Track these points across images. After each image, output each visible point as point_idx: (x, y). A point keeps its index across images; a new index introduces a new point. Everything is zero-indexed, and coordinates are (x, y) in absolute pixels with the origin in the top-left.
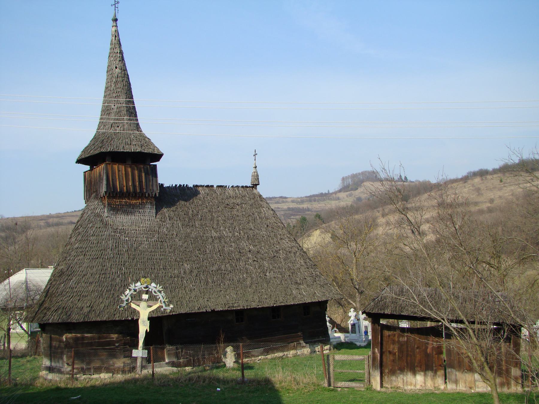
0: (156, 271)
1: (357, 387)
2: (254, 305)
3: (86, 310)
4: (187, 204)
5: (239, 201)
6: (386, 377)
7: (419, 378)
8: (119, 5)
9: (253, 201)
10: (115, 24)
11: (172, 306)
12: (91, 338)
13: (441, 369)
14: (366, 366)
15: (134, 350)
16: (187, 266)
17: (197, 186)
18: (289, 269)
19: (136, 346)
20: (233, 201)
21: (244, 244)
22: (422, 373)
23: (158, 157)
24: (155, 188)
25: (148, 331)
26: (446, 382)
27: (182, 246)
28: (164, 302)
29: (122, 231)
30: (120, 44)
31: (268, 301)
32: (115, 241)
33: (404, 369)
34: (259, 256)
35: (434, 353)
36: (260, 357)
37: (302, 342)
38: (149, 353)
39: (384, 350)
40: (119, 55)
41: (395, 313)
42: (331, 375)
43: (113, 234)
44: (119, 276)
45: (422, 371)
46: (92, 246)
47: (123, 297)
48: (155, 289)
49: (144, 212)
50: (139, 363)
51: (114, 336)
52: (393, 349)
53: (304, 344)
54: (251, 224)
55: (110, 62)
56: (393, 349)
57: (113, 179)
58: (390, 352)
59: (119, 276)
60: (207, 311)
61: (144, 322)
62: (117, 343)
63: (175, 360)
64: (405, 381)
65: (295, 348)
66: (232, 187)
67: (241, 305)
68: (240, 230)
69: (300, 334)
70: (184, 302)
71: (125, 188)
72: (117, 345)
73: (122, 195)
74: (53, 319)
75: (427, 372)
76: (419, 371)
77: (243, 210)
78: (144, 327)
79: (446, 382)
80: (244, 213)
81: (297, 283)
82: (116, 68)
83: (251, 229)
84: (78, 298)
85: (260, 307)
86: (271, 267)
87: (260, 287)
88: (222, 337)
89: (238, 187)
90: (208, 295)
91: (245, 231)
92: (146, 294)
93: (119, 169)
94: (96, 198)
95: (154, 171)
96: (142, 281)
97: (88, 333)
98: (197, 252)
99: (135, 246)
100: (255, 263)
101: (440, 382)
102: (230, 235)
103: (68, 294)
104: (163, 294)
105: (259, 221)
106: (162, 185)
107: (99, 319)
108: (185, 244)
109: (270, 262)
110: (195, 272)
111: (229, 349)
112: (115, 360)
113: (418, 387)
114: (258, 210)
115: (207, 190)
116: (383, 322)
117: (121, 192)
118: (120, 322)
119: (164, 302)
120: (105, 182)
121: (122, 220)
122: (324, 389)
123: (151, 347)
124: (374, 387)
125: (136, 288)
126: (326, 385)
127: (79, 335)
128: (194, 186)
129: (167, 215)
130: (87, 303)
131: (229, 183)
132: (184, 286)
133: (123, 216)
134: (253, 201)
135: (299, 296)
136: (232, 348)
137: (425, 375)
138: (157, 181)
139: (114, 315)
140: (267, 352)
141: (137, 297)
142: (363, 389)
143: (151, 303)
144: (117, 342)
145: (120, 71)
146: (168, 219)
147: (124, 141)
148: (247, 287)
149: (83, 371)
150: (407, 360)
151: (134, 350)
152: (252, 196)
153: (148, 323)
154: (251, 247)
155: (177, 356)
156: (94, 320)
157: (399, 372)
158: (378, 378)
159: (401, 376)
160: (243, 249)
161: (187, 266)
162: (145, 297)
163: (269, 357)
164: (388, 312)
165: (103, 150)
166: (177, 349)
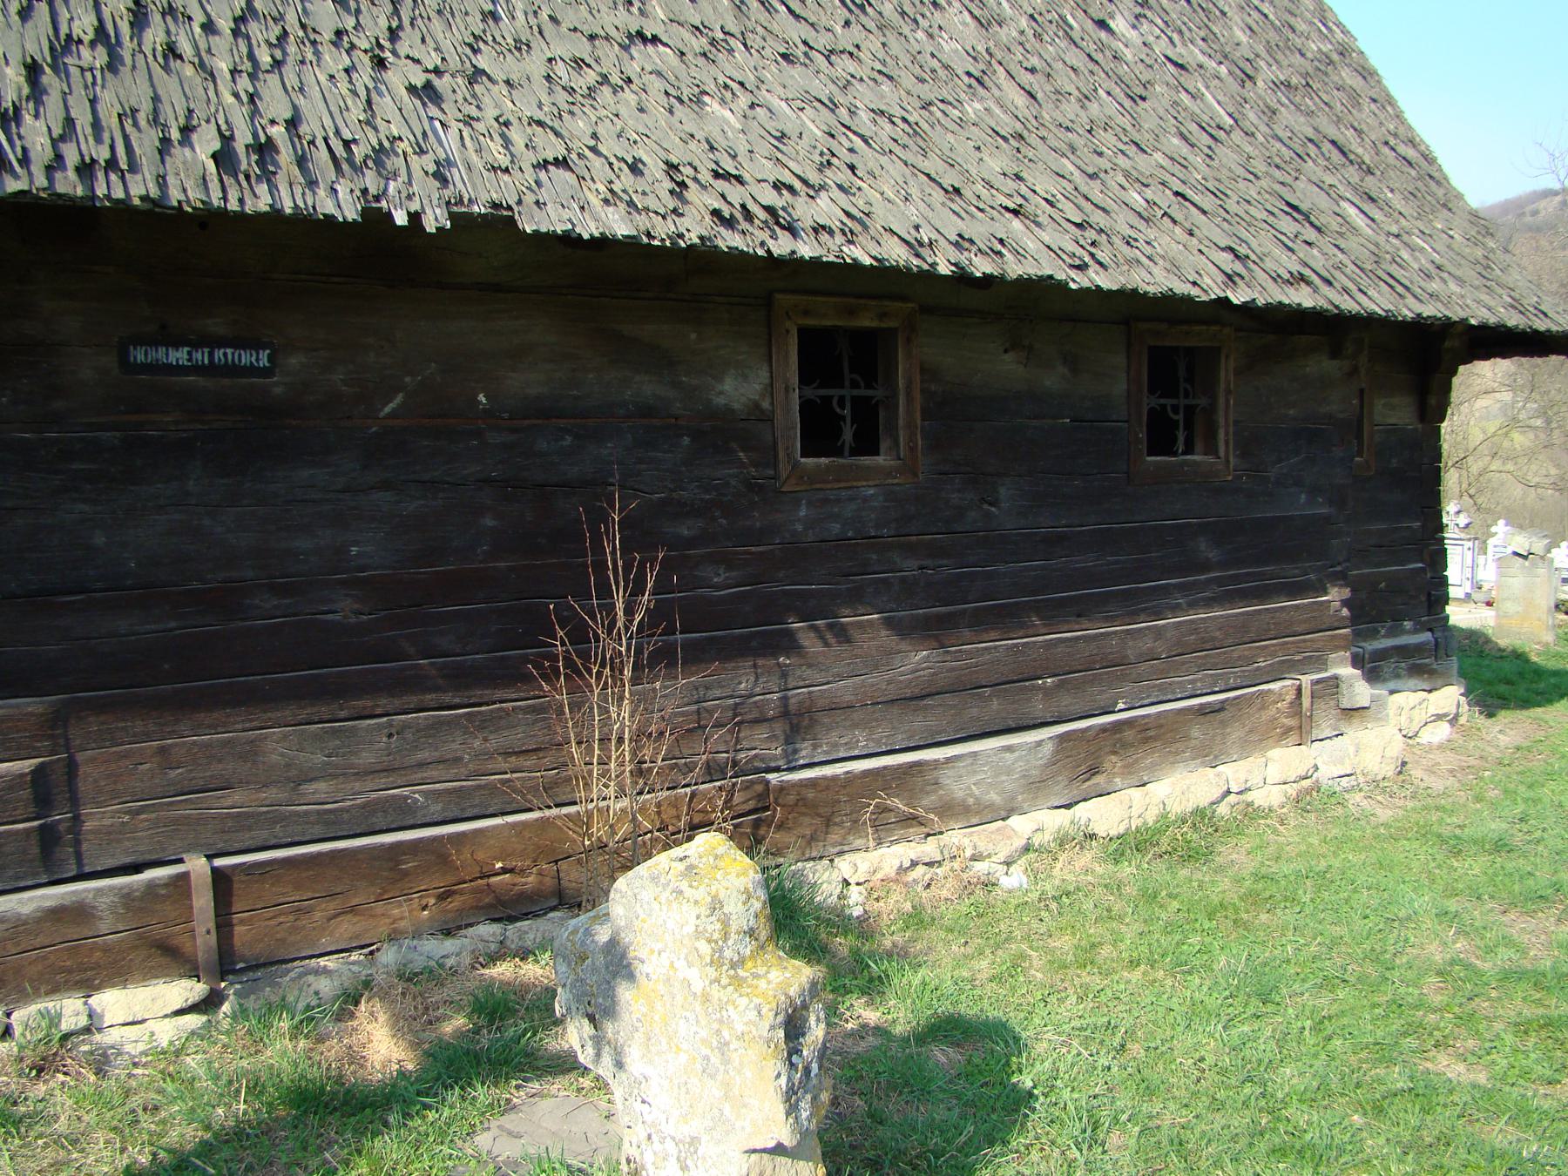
2: (1035, 254)
36: (1022, 826)
53: (1360, 691)
60: (374, 219)
65: (1299, 728)
69: (1335, 596)
85: (1106, 282)
88: (624, 616)
140: (1085, 766)
163: (1108, 814)
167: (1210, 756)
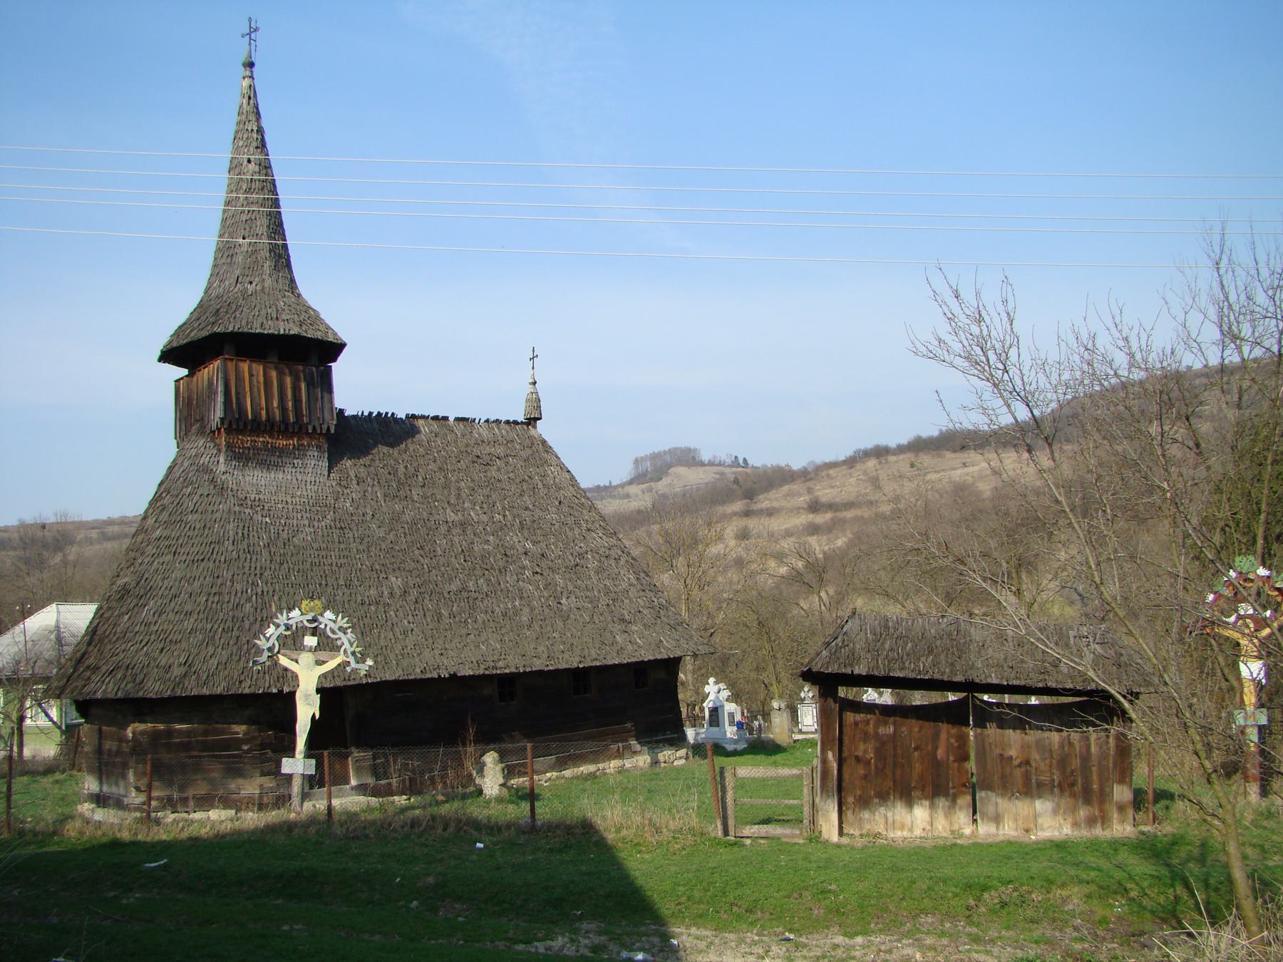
0: (330, 589)
1: (786, 836)
2: (538, 665)
3: (177, 671)
4: (395, 452)
5: (500, 451)
6: (849, 813)
7: (920, 813)
8: (258, 36)
9: (529, 451)
10: (248, 73)
11: (370, 662)
12: (188, 733)
13: (965, 793)
14: (806, 791)
15: (284, 760)
16: (396, 582)
17: (414, 416)
18: (607, 592)
19: (290, 751)
20: (488, 449)
21: (513, 538)
22: (927, 803)
23: (333, 349)
24: (327, 416)
25: (317, 716)
26: (975, 821)
27: (384, 539)
28: (353, 653)
29: (258, 504)
30: (258, 114)
31: (566, 656)
32: (241, 525)
33: (889, 794)
34: (544, 563)
35: (951, 758)
37: (633, 742)
38: (319, 766)
39: (845, 754)
40: (255, 136)
41: (876, 673)
42: (730, 812)
43: (237, 508)
44: (249, 600)
45: (926, 799)
46: (191, 533)
47: (262, 643)
48: (331, 625)
49: (305, 466)
50: (296, 788)
51: (240, 729)
52: (866, 751)
53: (638, 747)
54: (526, 498)
55: (236, 150)
56: (866, 751)
57: (237, 393)
58: (858, 759)
59: (249, 600)
61: (307, 696)
62: (246, 744)
63: (370, 781)
64: (890, 820)
65: (619, 755)
66: (487, 421)
67: (512, 663)
68: (504, 508)
69: (629, 725)
70: (392, 656)
71: (264, 412)
72: (245, 748)
73: (257, 427)
74: (105, 691)
75: (936, 801)
76: (919, 799)
77: (510, 469)
78: (307, 710)
79: (975, 821)
80: (511, 475)
81: (623, 620)
82: (249, 161)
83: (527, 509)
84: (161, 646)
86: (571, 587)
87: (549, 628)
89: (498, 422)
90: (441, 642)
91: (515, 511)
92: (313, 635)
93: (252, 372)
94: (201, 432)
95: (325, 383)
96: (303, 606)
97: (181, 722)
98: (417, 552)
99: (285, 535)
100: (538, 577)
101: (962, 819)
102: (485, 518)
103: (139, 638)
104: (350, 635)
105: (543, 492)
106: (341, 411)
107: (206, 691)
108: (392, 536)
109: (567, 576)
110: (414, 593)
111: (490, 758)
112: (241, 781)
113: (918, 832)
114: (540, 470)
115: (435, 425)
116: (842, 692)
117: (254, 419)
118: (254, 697)
119: (353, 653)
120: (220, 398)
121: (257, 481)
122: (716, 842)
123: (326, 753)
124: (825, 835)
125: (290, 622)
126: (720, 833)
127: (161, 727)
128: (407, 416)
129: (352, 474)
130: (179, 656)
131: (479, 411)
132: (389, 623)
133: (258, 473)
134: (529, 451)
135: (630, 647)
136: (496, 755)
137: (932, 806)
138: (331, 401)
139: (241, 682)
140: (561, 764)
141: (292, 641)
142: (801, 841)
143: (322, 655)
144: (246, 741)
145: (257, 168)
146: (355, 482)
147: (263, 312)
148: (522, 627)
149: (170, 804)
150: (894, 774)
151: (284, 760)
152: (527, 442)
153: (317, 699)
154: (529, 545)
155: (377, 772)
156: (195, 692)
157: (876, 800)
158: (834, 816)
159: (882, 810)
160: (513, 548)
161: (396, 582)
162: (311, 641)
163: (568, 773)
164: (860, 670)
165: (217, 329)
166: (375, 758)
167: (595, 761)
